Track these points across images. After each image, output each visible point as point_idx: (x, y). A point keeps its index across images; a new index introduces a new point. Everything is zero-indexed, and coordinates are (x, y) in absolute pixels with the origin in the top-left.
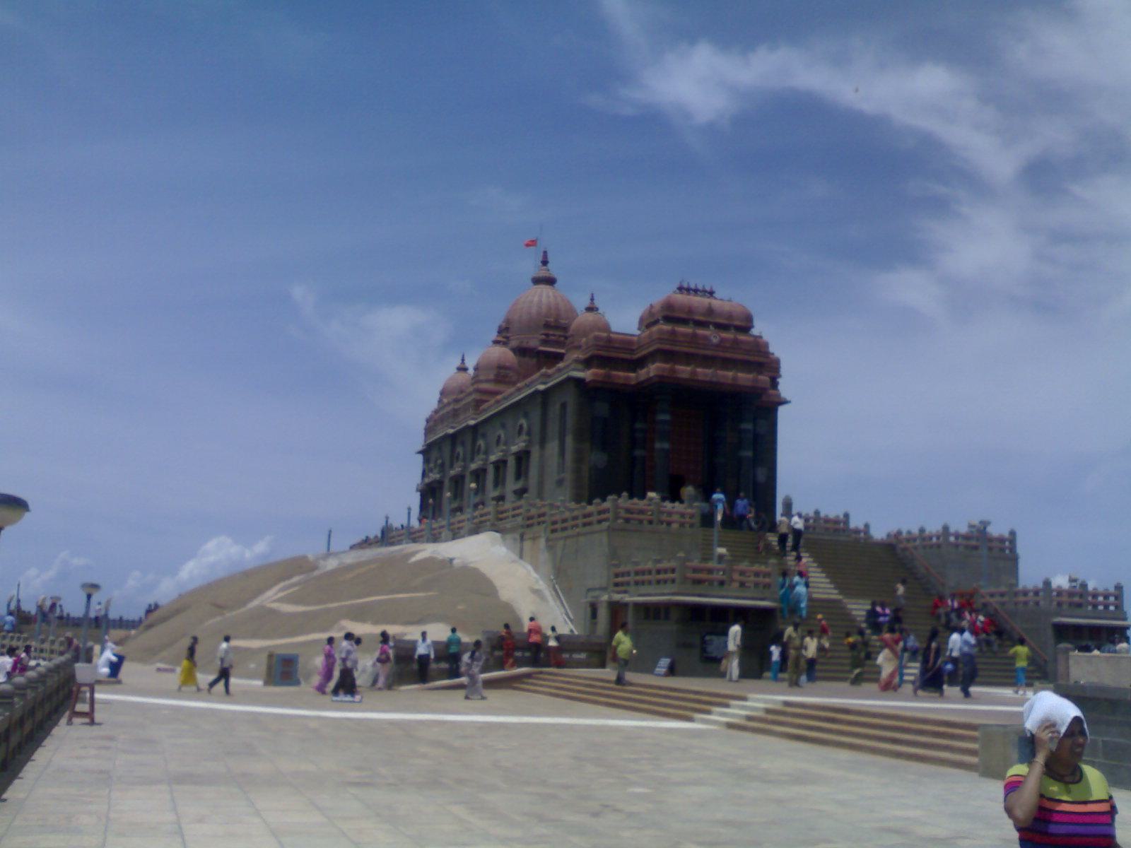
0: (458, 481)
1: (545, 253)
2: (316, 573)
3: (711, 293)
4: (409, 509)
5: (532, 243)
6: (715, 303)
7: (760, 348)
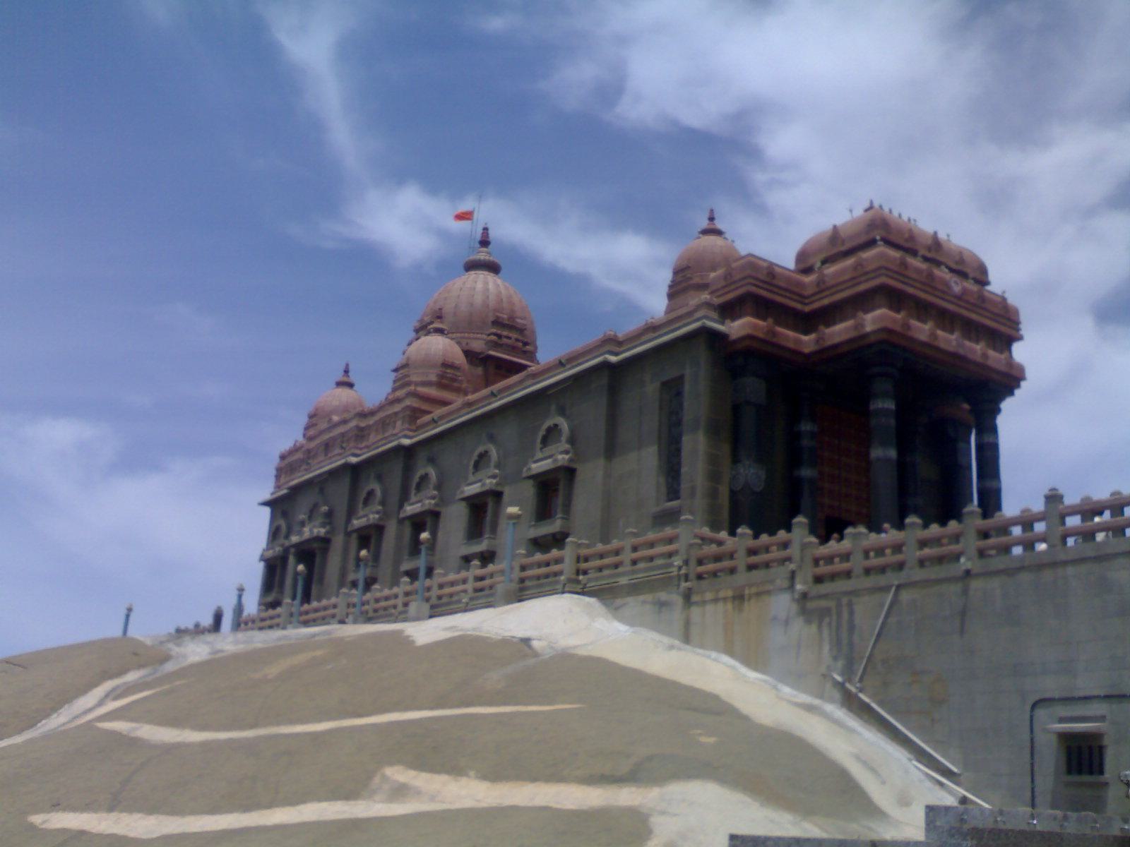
2: (170, 667)
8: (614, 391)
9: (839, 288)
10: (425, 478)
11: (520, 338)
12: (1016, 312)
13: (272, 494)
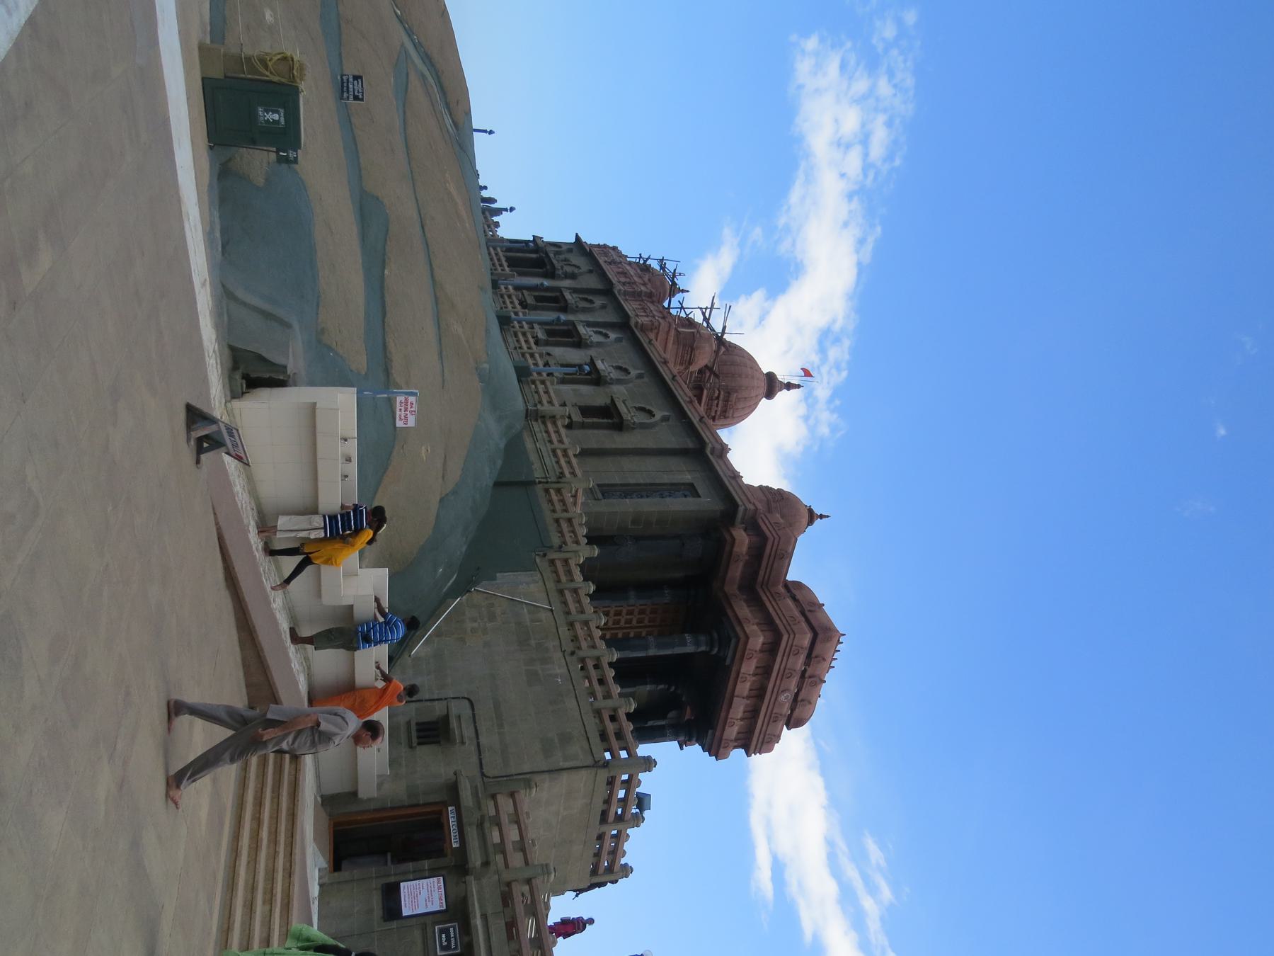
0: (555, 300)
5: (807, 373)
10: (606, 336)
12: (770, 750)
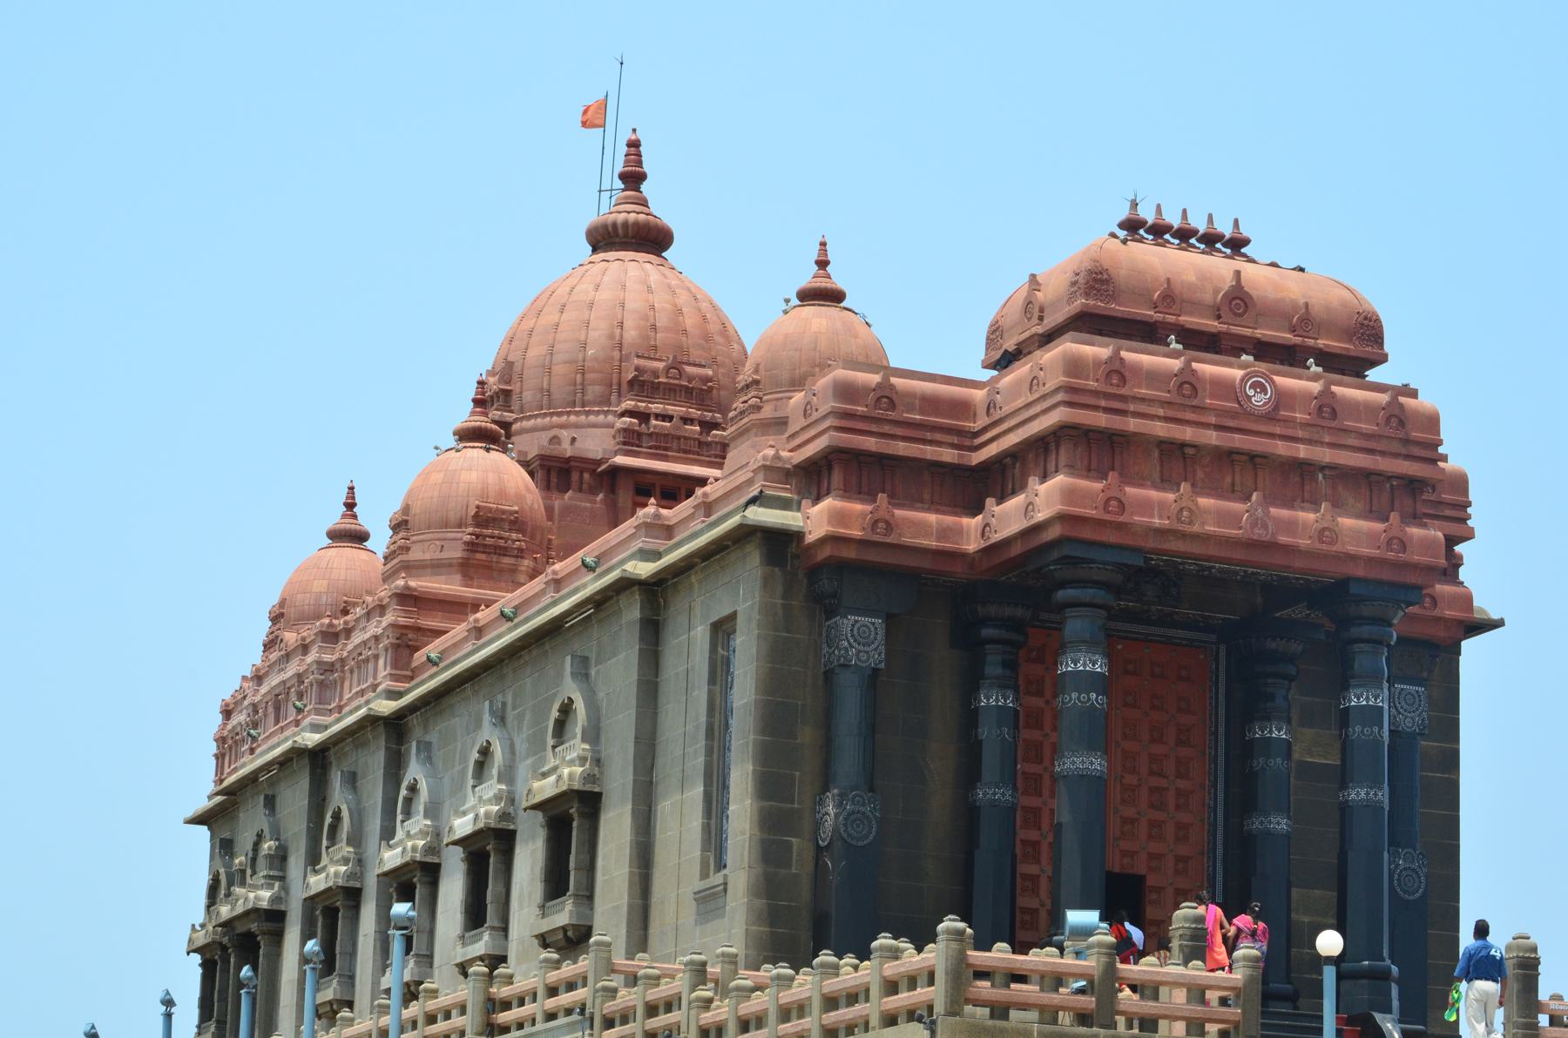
0: (333, 913)
1: (634, 145)
3: (1237, 245)
4: (168, 1002)
6: (1255, 276)
7: (1410, 430)
8: (653, 631)
9: (1005, 426)
11: (695, 413)
13: (210, 798)
